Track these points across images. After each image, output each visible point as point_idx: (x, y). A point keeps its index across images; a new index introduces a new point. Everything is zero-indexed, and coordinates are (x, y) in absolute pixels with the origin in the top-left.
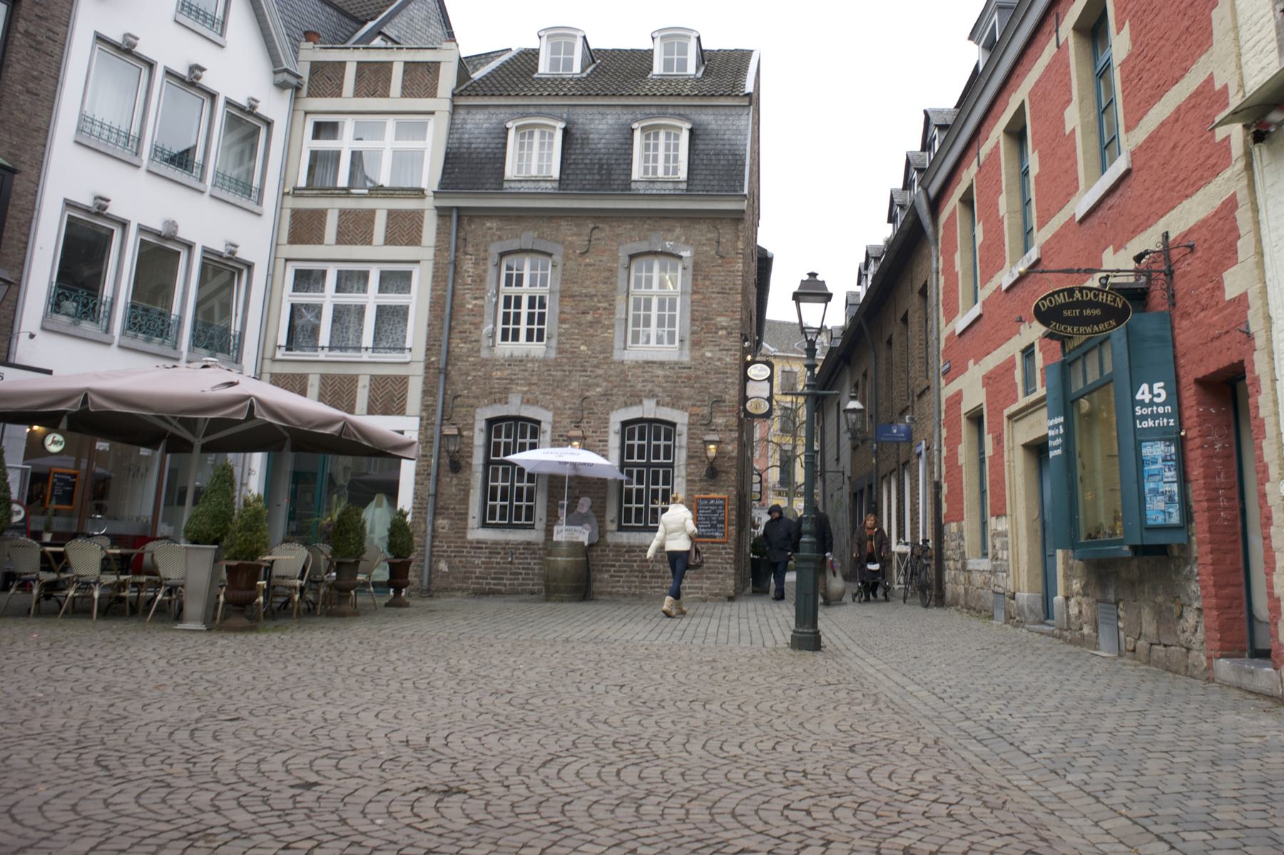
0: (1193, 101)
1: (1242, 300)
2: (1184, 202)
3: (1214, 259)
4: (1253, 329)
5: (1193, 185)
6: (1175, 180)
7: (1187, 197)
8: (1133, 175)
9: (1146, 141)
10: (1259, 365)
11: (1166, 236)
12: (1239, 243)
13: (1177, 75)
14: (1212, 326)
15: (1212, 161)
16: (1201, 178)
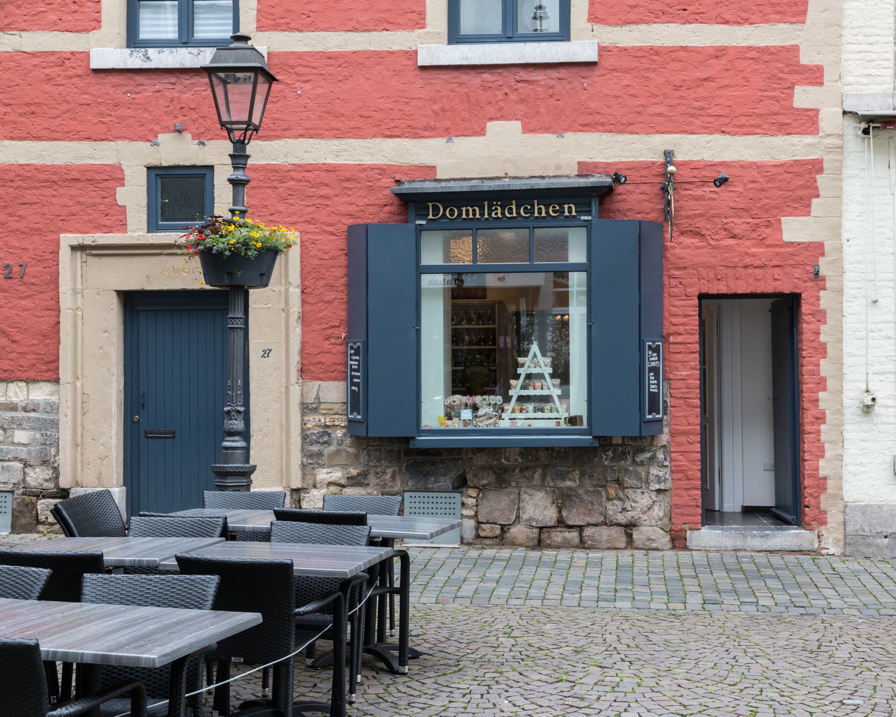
0: (753, 54)
1: (818, 249)
2: (718, 136)
3: (766, 201)
4: (823, 272)
5: (740, 126)
6: (702, 109)
7: (723, 132)
8: (598, 71)
9: (640, 49)
10: (825, 300)
11: (668, 154)
12: (815, 201)
13: (727, 16)
14: (754, 255)
15: (782, 119)
16: (758, 126)
